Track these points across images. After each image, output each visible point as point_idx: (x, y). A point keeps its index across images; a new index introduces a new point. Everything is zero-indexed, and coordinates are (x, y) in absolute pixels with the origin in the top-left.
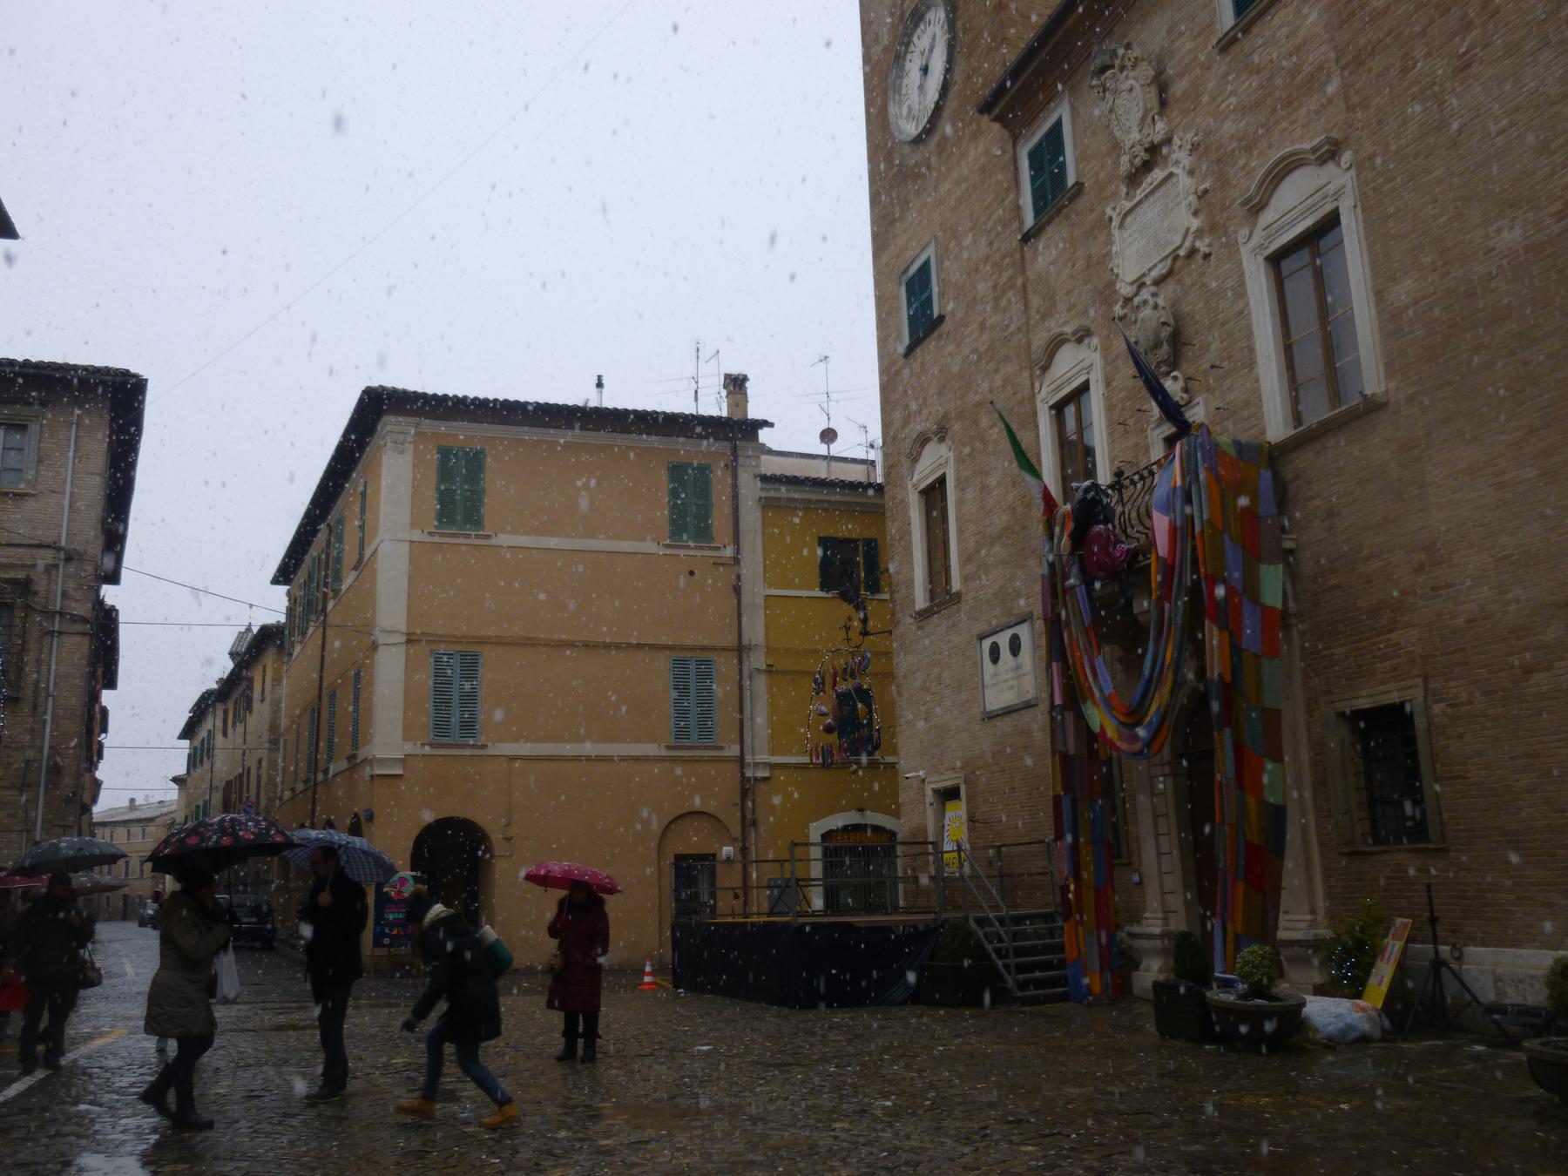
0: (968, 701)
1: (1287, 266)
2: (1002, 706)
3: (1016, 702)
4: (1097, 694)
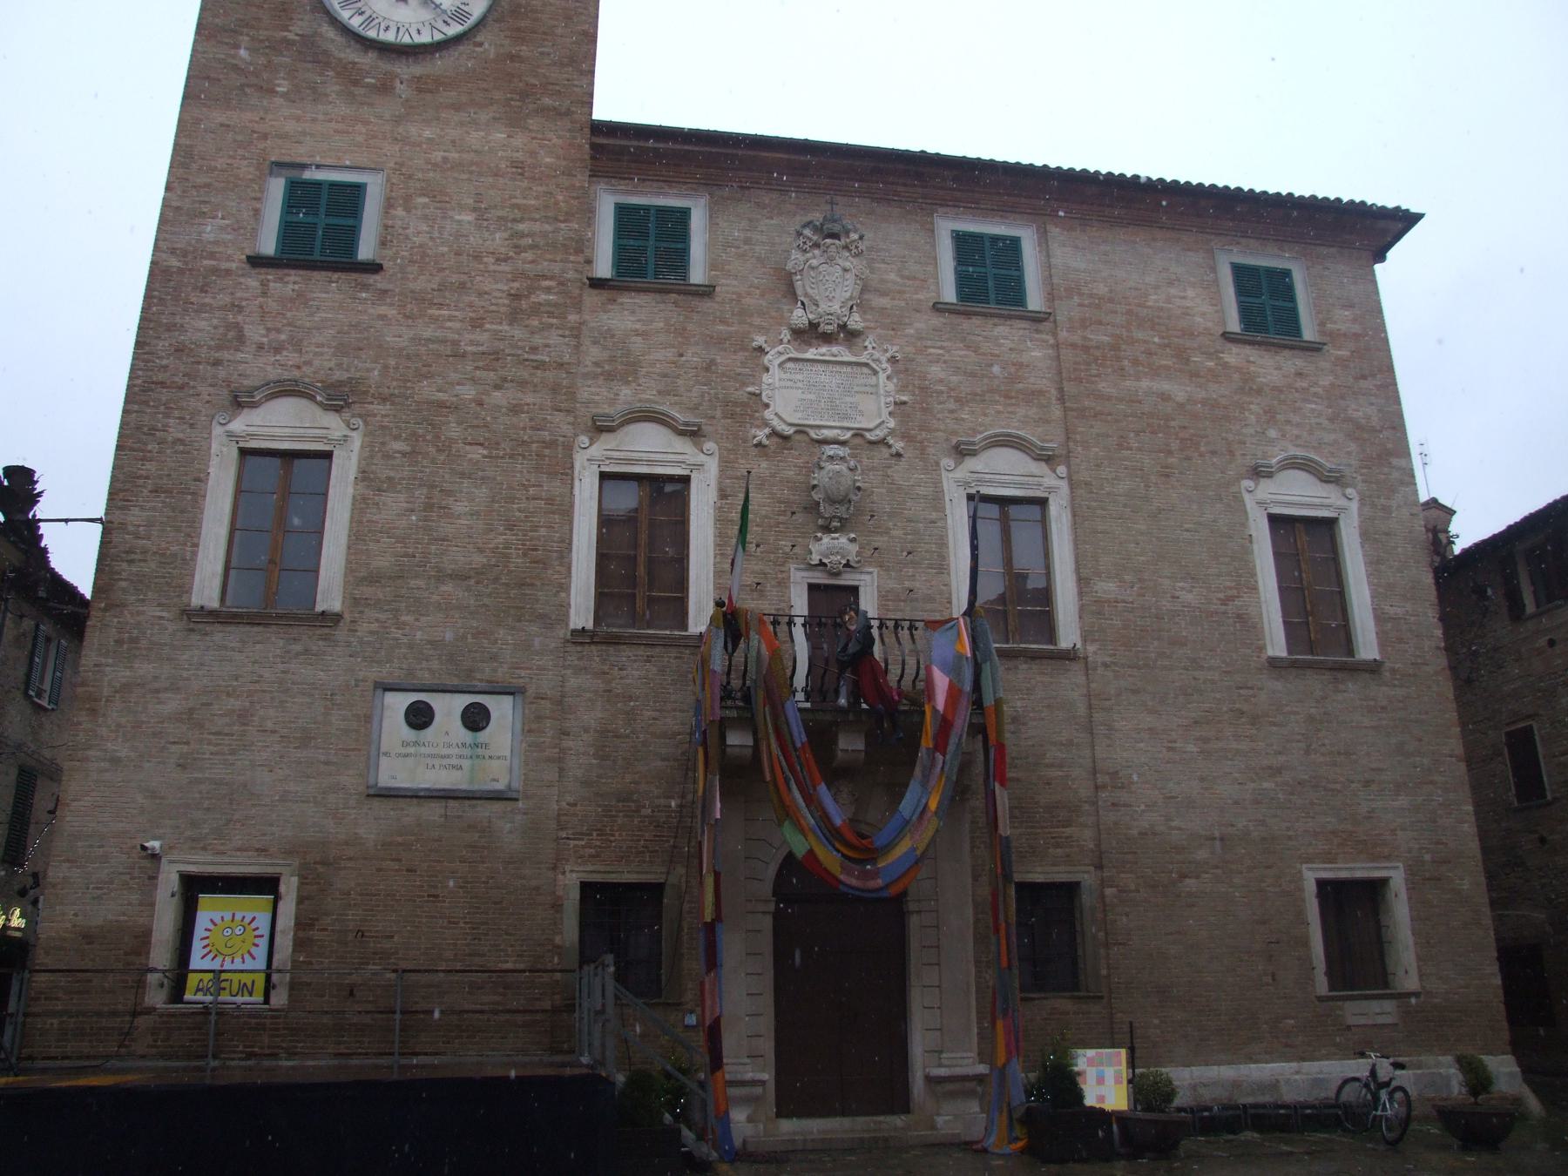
0: (327, 763)
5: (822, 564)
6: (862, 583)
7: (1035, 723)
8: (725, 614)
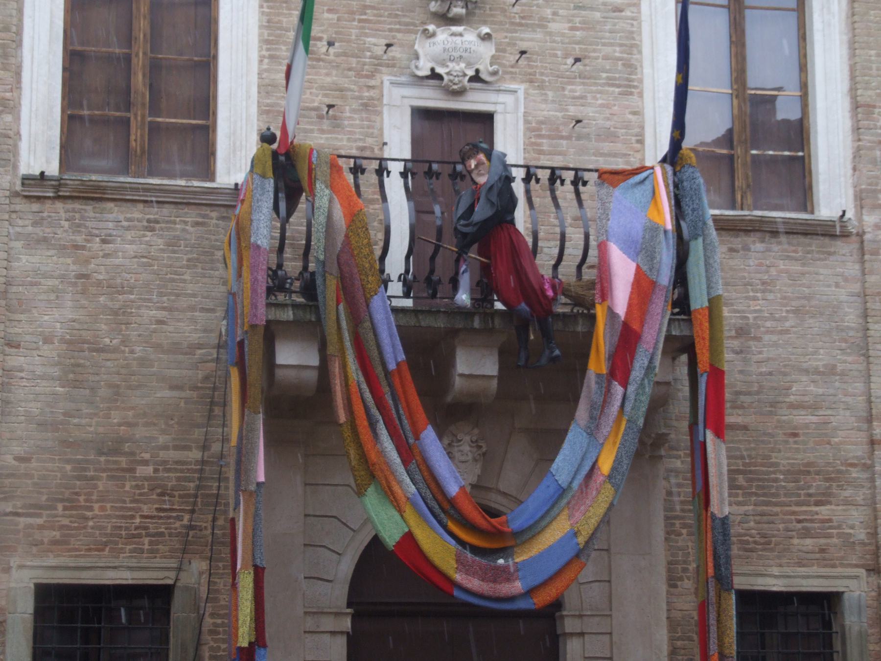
5: (435, 76)
6: (499, 108)
7: (774, 338)
8: (275, 154)
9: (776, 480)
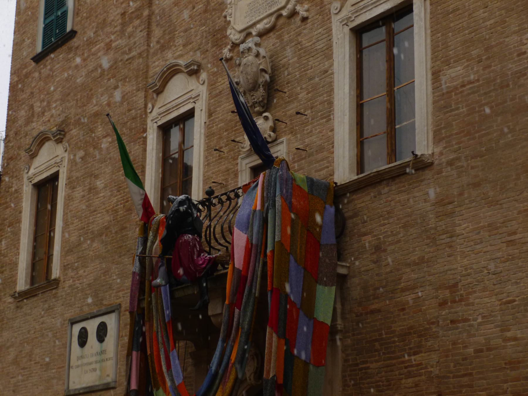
1: (367, 38)
2: (84, 385)
3: (97, 383)
4: (169, 383)
7: (393, 247)
9: (394, 342)
